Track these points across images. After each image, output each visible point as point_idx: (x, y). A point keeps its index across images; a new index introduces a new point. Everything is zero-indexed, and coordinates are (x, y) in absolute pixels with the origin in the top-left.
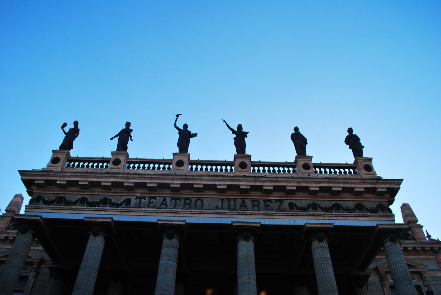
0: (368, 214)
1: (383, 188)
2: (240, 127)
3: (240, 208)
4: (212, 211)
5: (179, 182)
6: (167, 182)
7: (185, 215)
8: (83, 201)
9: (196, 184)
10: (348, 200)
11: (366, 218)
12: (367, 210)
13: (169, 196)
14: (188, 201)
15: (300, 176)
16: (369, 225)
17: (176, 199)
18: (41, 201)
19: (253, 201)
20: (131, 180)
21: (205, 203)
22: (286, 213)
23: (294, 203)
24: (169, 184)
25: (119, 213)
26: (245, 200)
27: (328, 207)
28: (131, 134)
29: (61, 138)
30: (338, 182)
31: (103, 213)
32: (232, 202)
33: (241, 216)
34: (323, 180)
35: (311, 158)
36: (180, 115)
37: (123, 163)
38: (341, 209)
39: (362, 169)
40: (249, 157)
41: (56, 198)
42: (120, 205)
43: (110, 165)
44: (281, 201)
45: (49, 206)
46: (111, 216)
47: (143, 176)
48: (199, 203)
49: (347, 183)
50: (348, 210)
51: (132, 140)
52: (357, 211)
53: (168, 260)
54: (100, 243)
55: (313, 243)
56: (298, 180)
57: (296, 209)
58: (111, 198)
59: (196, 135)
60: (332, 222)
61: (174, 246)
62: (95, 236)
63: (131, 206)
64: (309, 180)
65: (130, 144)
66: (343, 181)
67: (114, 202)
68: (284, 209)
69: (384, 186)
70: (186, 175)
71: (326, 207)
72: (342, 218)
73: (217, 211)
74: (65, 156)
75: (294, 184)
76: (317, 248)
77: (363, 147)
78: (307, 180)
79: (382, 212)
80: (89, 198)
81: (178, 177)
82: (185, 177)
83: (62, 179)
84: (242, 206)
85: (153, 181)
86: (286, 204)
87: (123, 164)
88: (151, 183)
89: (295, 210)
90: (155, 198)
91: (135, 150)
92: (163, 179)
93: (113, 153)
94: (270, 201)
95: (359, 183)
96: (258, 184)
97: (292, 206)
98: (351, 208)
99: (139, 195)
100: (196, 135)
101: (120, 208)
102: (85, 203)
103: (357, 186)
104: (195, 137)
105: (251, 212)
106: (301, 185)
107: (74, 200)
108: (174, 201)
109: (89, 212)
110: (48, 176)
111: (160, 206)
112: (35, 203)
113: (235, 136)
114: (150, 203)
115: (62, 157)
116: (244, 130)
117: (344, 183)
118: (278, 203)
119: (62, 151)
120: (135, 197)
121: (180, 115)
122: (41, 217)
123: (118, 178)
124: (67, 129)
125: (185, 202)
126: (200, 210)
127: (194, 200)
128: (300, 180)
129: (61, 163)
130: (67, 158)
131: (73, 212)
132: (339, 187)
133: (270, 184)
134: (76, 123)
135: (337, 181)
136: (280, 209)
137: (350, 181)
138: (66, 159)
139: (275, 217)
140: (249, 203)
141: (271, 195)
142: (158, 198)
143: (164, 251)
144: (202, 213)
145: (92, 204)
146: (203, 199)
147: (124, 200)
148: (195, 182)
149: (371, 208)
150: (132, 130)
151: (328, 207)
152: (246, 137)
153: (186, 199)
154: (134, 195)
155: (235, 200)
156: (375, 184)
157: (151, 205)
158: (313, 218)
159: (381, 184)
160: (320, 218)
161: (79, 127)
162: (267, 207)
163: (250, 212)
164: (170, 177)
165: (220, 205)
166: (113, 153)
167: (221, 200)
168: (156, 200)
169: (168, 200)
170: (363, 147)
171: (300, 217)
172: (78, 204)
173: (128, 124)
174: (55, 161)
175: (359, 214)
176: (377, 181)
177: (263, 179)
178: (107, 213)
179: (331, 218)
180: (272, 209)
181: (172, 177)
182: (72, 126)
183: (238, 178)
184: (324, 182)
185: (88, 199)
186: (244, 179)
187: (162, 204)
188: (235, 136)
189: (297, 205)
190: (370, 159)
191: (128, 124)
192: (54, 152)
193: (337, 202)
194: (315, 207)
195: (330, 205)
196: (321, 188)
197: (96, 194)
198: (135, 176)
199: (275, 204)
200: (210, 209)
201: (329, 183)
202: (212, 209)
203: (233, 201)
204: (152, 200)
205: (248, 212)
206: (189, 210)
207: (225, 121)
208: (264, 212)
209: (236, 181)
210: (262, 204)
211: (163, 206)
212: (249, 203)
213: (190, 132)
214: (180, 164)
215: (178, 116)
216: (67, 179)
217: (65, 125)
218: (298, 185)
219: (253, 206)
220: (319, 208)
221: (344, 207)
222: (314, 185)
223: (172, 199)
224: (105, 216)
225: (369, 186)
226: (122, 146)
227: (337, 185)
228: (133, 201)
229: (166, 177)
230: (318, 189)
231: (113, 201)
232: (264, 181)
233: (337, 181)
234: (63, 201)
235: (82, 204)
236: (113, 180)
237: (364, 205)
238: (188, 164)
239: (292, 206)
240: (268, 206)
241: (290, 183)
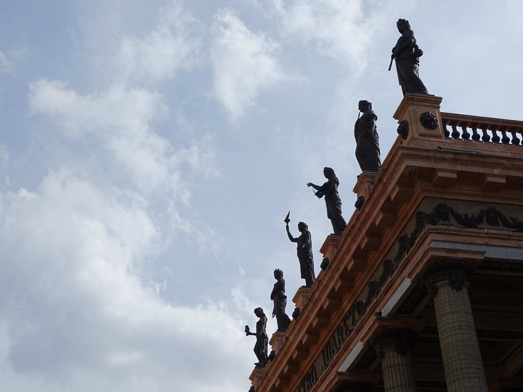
1: (394, 189)
30: (358, 229)
36: (288, 216)
103: (375, 214)
121: (288, 216)
132: (363, 238)
139: (352, 346)
141: (342, 308)
215: (287, 220)
227: (361, 236)
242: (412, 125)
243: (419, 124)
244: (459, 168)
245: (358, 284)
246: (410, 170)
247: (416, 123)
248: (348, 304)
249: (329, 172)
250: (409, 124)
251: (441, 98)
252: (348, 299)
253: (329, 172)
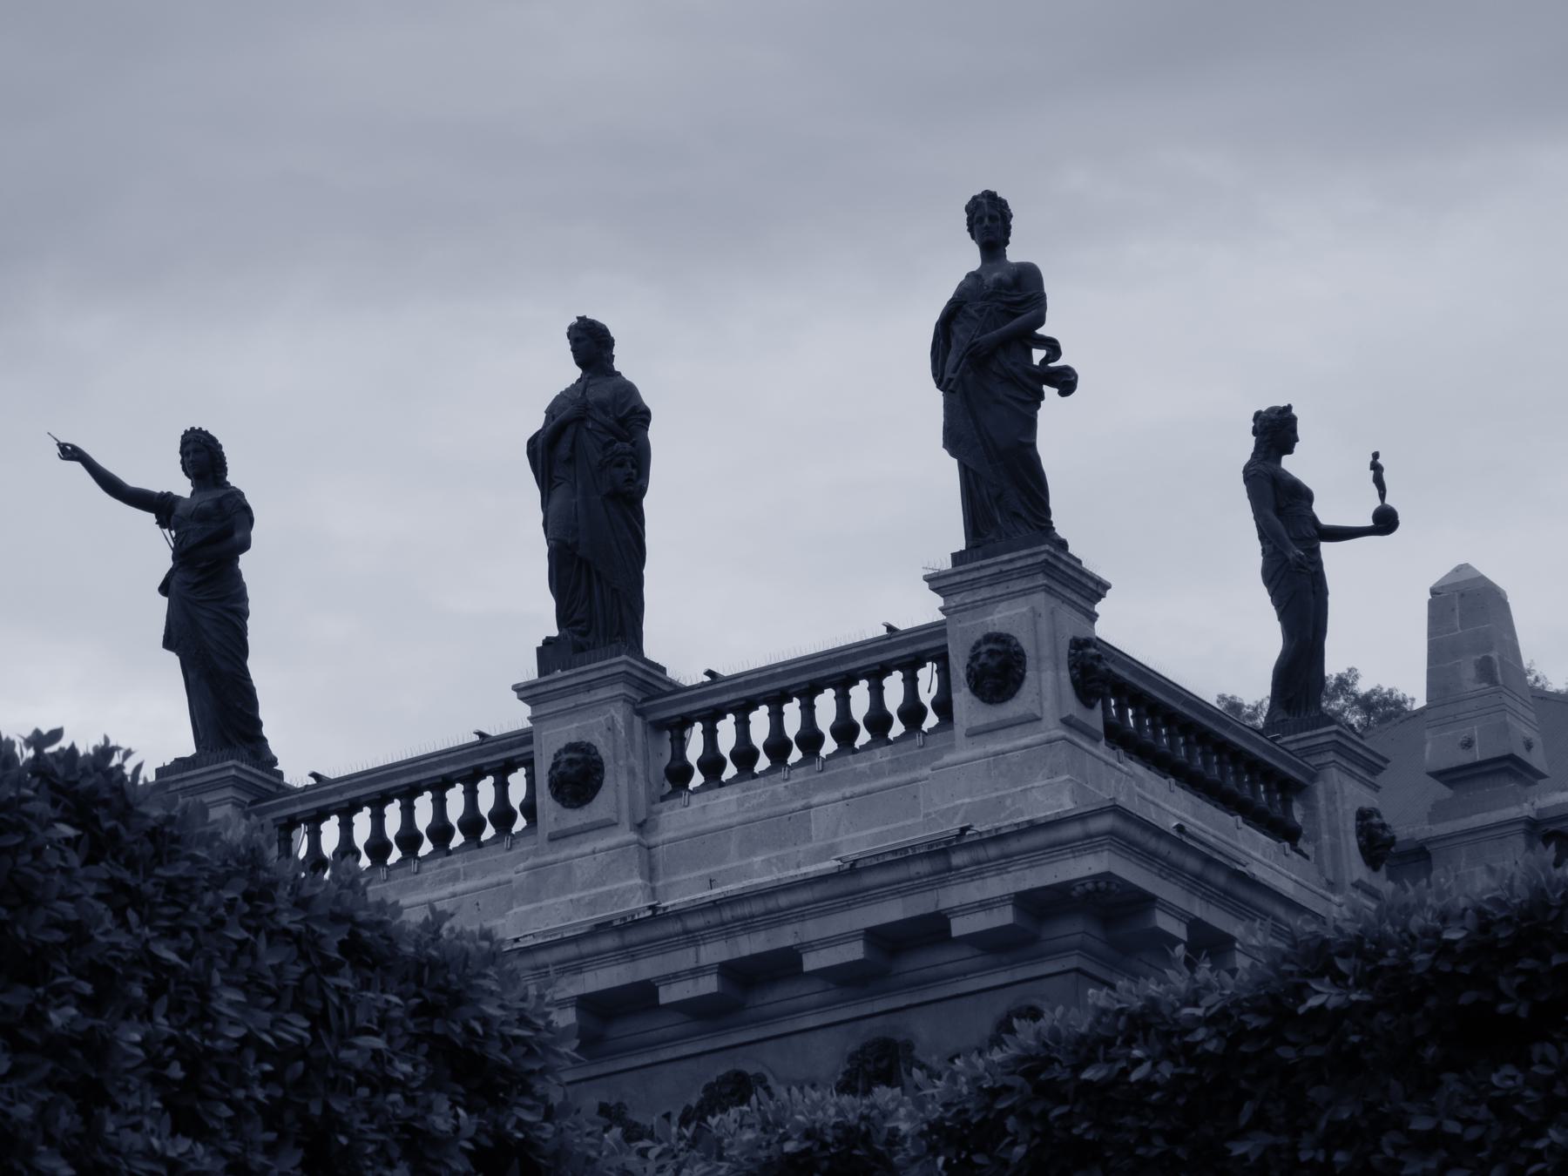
1: (985, 905)
10: (811, 1021)
30: (686, 932)
34: (588, 947)
49: (748, 925)
103: (812, 929)
117: (726, 930)
132: (697, 972)
135: (678, 927)
137: (757, 907)
156: (931, 886)
159: (972, 877)
176: (939, 863)
184: (599, 959)
201: (628, 953)
207: (70, 453)
227: (683, 959)
233: (678, 927)
242: (1039, 670)
243: (1065, 675)
244: (1199, 909)
246: (1102, 885)
247: (1057, 667)
249: (202, 455)
250: (1030, 663)
251: (1106, 587)
253: (202, 455)
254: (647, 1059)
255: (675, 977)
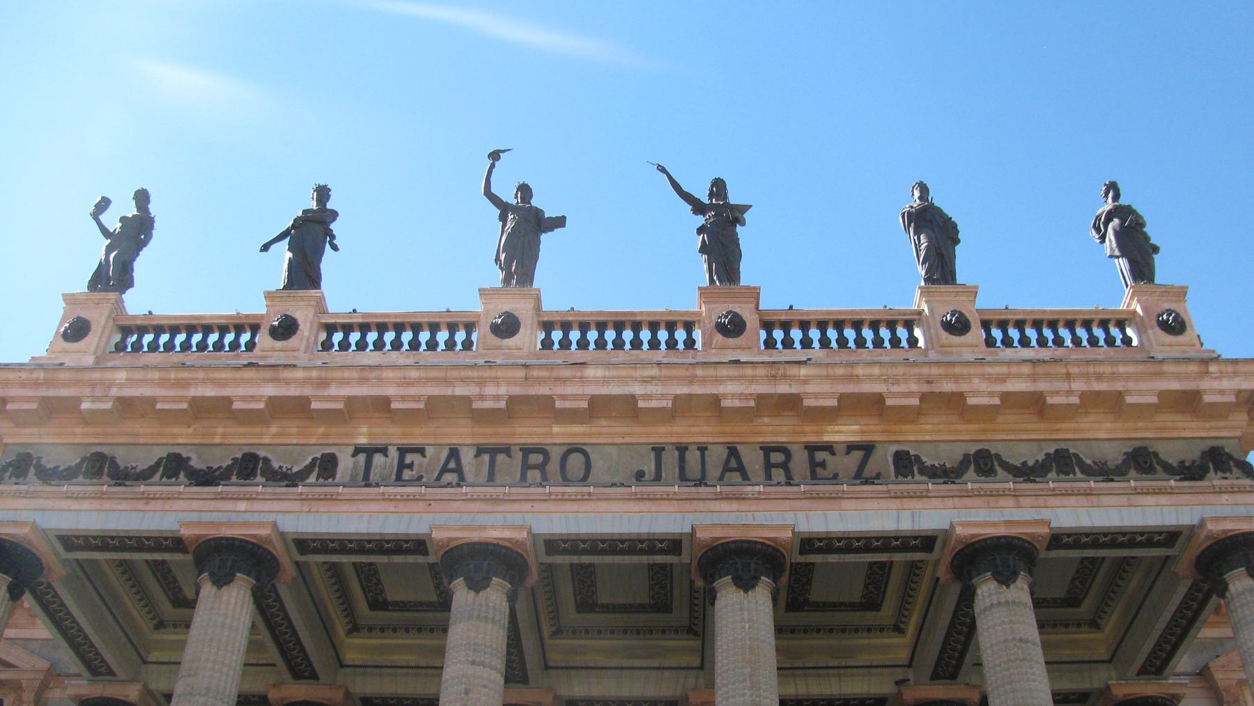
0: (1172, 483)
1: (1222, 392)
2: (719, 187)
3: (721, 478)
4: (622, 490)
5: (503, 390)
6: (460, 391)
7: (527, 506)
8: (174, 466)
9: (564, 397)
11: (1164, 500)
12: (1169, 470)
13: (469, 441)
14: (536, 458)
15: (933, 356)
16: (1174, 523)
17: (494, 451)
18: (32, 470)
19: (767, 450)
20: (333, 391)
21: (598, 463)
22: (883, 488)
23: (912, 453)
24: (467, 400)
25: (295, 506)
26: (739, 447)
27: (1030, 463)
28: (333, 226)
29: (95, 250)
31: (242, 506)
32: (693, 457)
33: (725, 506)
34: (1014, 370)
35: (973, 292)
36: (503, 151)
37: (305, 329)
38: (1077, 470)
39: (1152, 328)
40: (754, 294)
41: (84, 459)
42: (302, 476)
43: (263, 339)
44: (867, 449)
45: (59, 489)
46: (272, 518)
47: (374, 374)
48: (576, 461)
50: (1103, 472)
51: (335, 248)
52: (1133, 473)
53: (473, 663)
54: (238, 610)
55: (979, 592)
56: (925, 370)
57: (921, 473)
58: (269, 456)
59: (560, 222)
60: (1045, 514)
61: (490, 616)
62: (220, 587)
63: (338, 476)
64: (965, 370)
65: (329, 263)
66: (1084, 370)
67: (281, 467)
68: (878, 476)
69: (1226, 384)
70: (526, 366)
71: (1024, 464)
72: (1082, 500)
73: (639, 489)
74: (106, 313)
75: (914, 387)
76: (992, 605)
77: (1155, 249)
78: (957, 370)
79: (1220, 474)
80: (194, 456)
81: (500, 373)
82: (521, 373)
83: (99, 392)
84: (726, 469)
85: (413, 391)
86: (883, 459)
87: (306, 334)
88: (403, 398)
89: (918, 477)
90: (421, 451)
91: (347, 286)
92: (447, 381)
93: (269, 296)
94: (829, 448)
95: (1139, 377)
96: (783, 388)
97: (905, 463)
98: (1111, 465)
99: (363, 441)
100: (560, 222)
101: (300, 489)
102: (182, 475)
103: (1131, 385)
104: (558, 231)
105: (761, 488)
106: (937, 388)
107: (142, 466)
108: (486, 457)
109: (196, 505)
110: (49, 383)
111: (438, 478)
112: (10, 477)
113: (700, 220)
114: (402, 466)
115: (99, 318)
116: (734, 199)
118: (857, 455)
119: (97, 296)
120: (352, 449)
121: (503, 151)
122: (34, 526)
123: (287, 382)
124: (112, 221)
125: (525, 458)
126: (579, 489)
127: (556, 454)
128: (935, 371)
129: (96, 339)
130: (114, 320)
131: (141, 505)
132: (1069, 393)
133: (826, 388)
134: (142, 198)
136: (860, 476)
138: (111, 323)
139: (846, 504)
140: (753, 460)
141: (829, 428)
142: (430, 451)
143: (458, 633)
144: (589, 498)
145: (205, 478)
146: (587, 449)
147: (314, 460)
148: (560, 390)
149: (1182, 462)
150: (334, 215)
151: (1030, 463)
152: (743, 223)
153: (527, 451)
154: (346, 441)
155: (703, 449)
156: (1195, 379)
157: (407, 474)
158: (978, 501)
160: (1002, 502)
161: (153, 208)
162: (816, 470)
163: (757, 488)
164: (468, 373)
165: (650, 468)
166: (269, 296)
167: (653, 449)
168: (424, 456)
169: (467, 457)
170: (1155, 249)
171: (935, 502)
172: (158, 475)
173: (323, 193)
174: (76, 331)
175: (1139, 484)
176: (1203, 368)
177: (803, 371)
178: (258, 506)
179: (1041, 501)
180: (835, 476)
181: (475, 374)
182: (131, 211)
183: (710, 372)
184: (1019, 376)
185: (189, 459)
186: (733, 371)
187: (444, 470)
188: (700, 220)
189: (924, 459)
190: (1181, 293)
191: (323, 193)
192: (70, 299)
193: (1062, 446)
194: (984, 462)
195: (1041, 457)
196: (1005, 396)
197: (217, 440)
198: (346, 374)
199: (846, 459)
200: (613, 485)
201: (1034, 378)
202: (622, 485)
203: (698, 453)
204: (409, 458)
205: (749, 488)
206: (540, 490)
207: (663, 170)
208: (807, 488)
209: (703, 381)
210: (800, 460)
211: (450, 477)
212: (753, 460)
213: (538, 213)
214: (507, 327)
215: (495, 156)
216: (115, 392)
217: (103, 205)
218: (926, 388)
219: (768, 466)
220: (999, 469)
221: (1089, 462)
222: (984, 386)
223: (480, 450)
224: (249, 517)
225: (1175, 385)
226: (304, 273)
227: (1064, 386)
228: (346, 463)
229: (455, 374)
230: (996, 401)
231: (276, 465)
232: (806, 381)
234: (106, 470)
235: (169, 477)
236: (270, 391)
237: (1155, 454)
238: (535, 325)
239: (905, 463)
240: (823, 465)
241: (897, 382)
245: (929, 427)
248: (854, 432)
252: (865, 428)
254: (1013, 437)
255: (1057, 393)
